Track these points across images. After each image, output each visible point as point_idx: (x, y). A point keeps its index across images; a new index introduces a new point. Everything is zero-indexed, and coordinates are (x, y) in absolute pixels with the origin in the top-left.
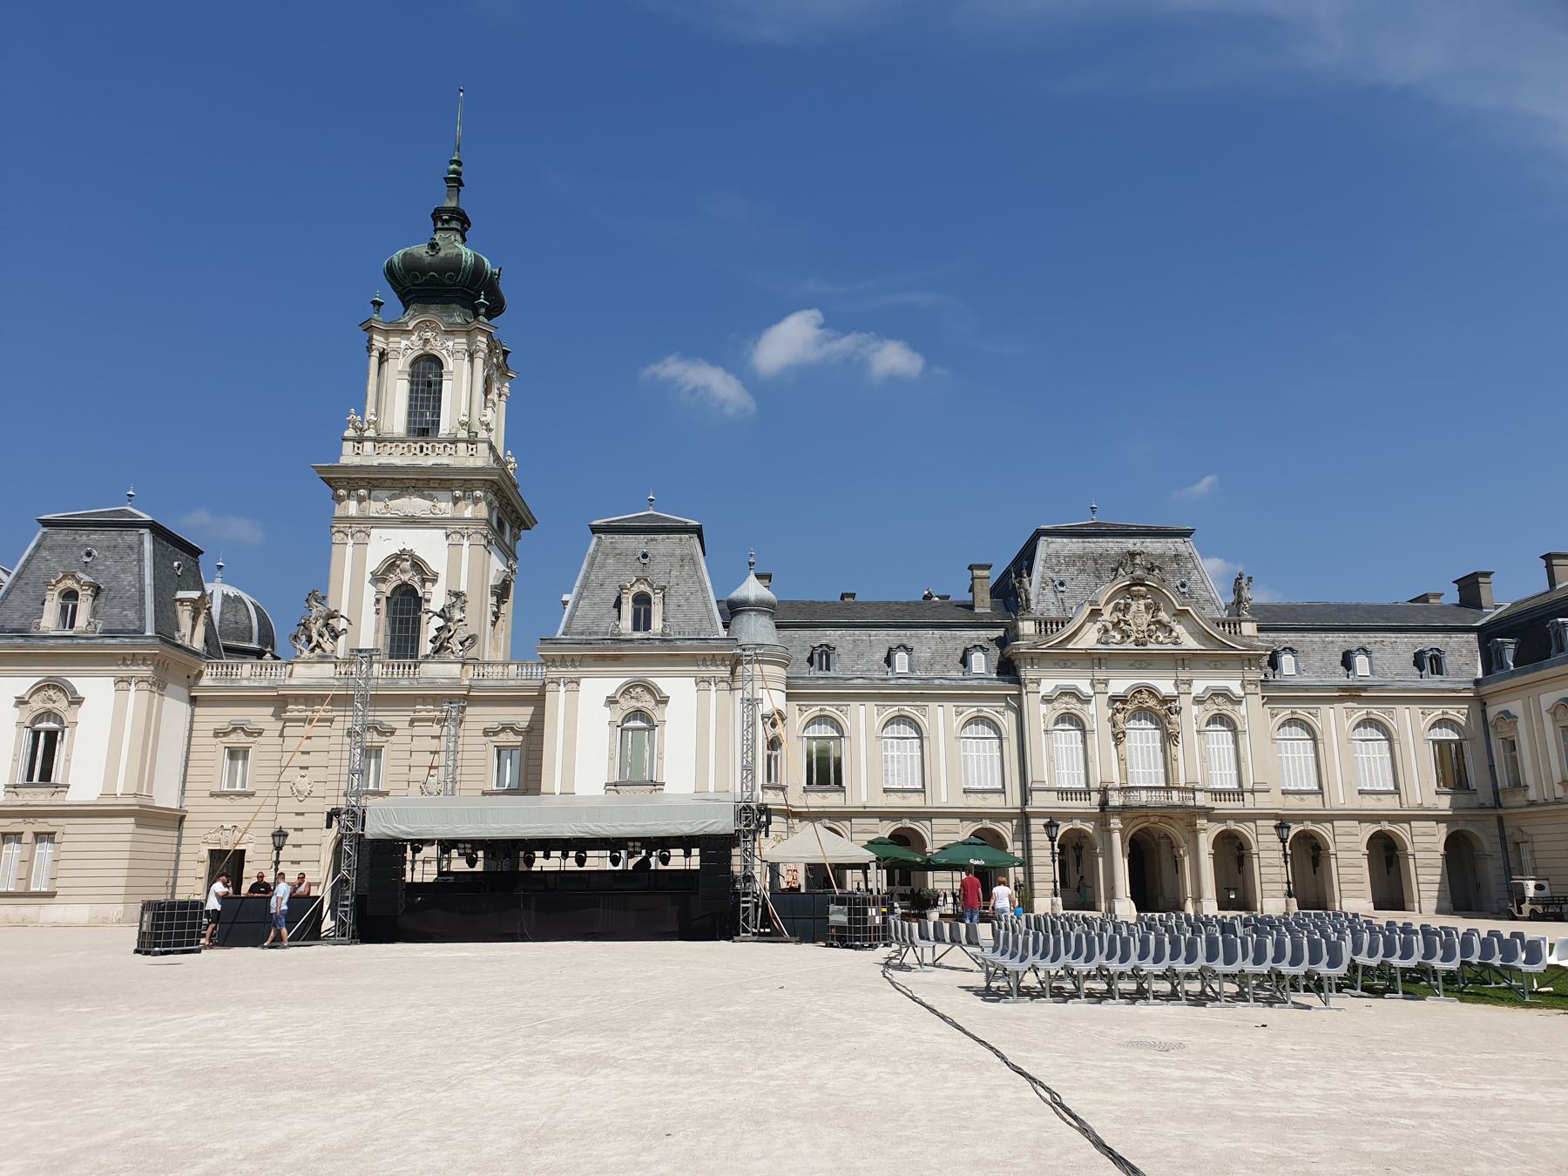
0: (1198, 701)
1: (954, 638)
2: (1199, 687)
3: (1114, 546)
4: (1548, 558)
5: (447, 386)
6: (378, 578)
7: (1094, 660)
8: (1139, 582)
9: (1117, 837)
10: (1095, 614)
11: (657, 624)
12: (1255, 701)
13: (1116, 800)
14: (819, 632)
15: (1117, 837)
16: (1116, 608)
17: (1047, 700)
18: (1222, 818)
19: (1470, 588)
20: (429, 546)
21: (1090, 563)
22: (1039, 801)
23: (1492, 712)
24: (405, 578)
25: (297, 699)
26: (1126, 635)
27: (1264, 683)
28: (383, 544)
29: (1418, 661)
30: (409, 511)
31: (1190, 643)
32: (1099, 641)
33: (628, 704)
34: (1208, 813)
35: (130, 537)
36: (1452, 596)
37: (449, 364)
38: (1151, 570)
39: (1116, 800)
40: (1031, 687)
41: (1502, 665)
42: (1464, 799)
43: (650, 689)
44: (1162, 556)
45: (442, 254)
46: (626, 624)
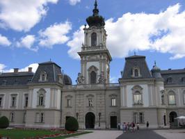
6: (89, 70)
11: (139, 75)
20: (97, 64)
28: (89, 64)
37: (98, 34)
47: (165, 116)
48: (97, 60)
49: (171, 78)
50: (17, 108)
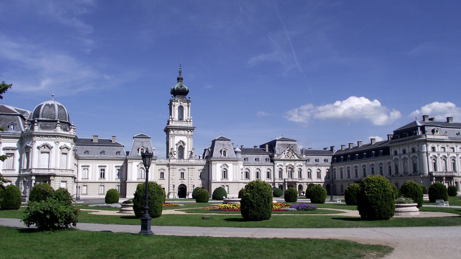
1: (264, 156)
2: (297, 164)
3: (286, 142)
6: (177, 145)
9: (286, 185)
10: (285, 153)
13: (286, 181)
14: (245, 155)
15: (286, 185)
18: (300, 183)
19: (332, 148)
20: (184, 139)
21: (283, 145)
22: (276, 181)
23: (333, 168)
24: (181, 144)
25: (171, 165)
27: (306, 164)
30: (181, 133)
31: (297, 158)
32: (285, 158)
33: (224, 167)
34: (298, 182)
35: (148, 140)
38: (292, 147)
39: (286, 181)
43: (226, 165)
44: (293, 144)
45: (183, 88)
46: (223, 155)
48: (184, 135)
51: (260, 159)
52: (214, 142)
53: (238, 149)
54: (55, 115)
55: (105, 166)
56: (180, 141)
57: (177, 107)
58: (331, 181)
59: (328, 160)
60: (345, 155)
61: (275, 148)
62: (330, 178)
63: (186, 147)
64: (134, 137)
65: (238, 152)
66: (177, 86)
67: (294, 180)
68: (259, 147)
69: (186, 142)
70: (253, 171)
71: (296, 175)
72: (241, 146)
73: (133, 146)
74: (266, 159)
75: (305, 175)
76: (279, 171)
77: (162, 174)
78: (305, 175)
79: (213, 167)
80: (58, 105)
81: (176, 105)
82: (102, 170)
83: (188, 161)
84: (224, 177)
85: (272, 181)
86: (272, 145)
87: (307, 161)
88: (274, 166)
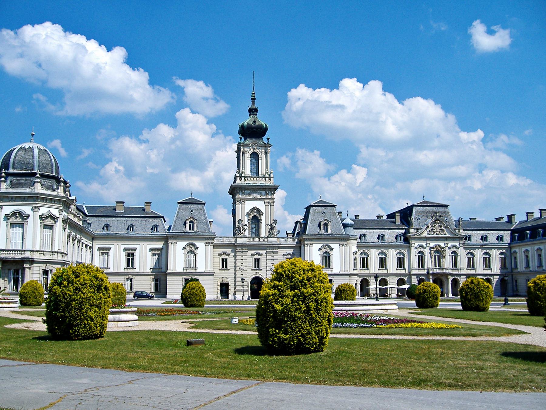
0: (449, 248)
2: (449, 245)
3: (430, 209)
4: (527, 213)
5: (260, 161)
6: (248, 214)
7: (427, 238)
8: (438, 220)
9: (431, 280)
10: (428, 227)
11: (329, 231)
12: (462, 248)
13: (431, 272)
16: (432, 226)
17: (416, 248)
19: (510, 217)
20: (260, 205)
21: (425, 214)
23: (513, 250)
26: (434, 232)
28: (249, 205)
29: (498, 239)
31: (448, 235)
33: (324, 250)
34: (451, 275)
35: (200, 207)
36: (506, 219)
38: (440, 216)
39: (431, 272)
40: (413, 245)
41: (515, 240)
42: (505, 271)
43: (329, 247)
44: (442, 212)
45: (257, 124)
46: (322, 231)
47: (356, 284)
49: (365, 235)
50: (137, 271)
51: (386, 237)
52: (308, 209)
53: (348, 221)
54: (33, 165)
55: (135, 249)
56: (254, 208)
57: (247, 155)
58: (508, 272)
59: (504, 238)
60: (534, 230)
61: (411, 218)
62: (507, 267)
63: (263, 218)
64: (179, 203)
65: (348, 224)
66: (248, 120)
67: (444, 271)
68: (385, 217)
69: (263, 210)
70: (374, 256)
71: (447, 262)
72: (356, 216)
73: (177, 217)
74: (397, 236)
75: (462, 262)
76: (419, 256)
77: (225, 262)
78: (462, 262)
79: (307, 249)
80: (39, 149)
81: (248, 151)
82: (129, 255)
83: (266, 240)
84: (326, 266)
85: (407, 272)
86: (406, 214)
87: (466, 239)
88: (409, 247)
